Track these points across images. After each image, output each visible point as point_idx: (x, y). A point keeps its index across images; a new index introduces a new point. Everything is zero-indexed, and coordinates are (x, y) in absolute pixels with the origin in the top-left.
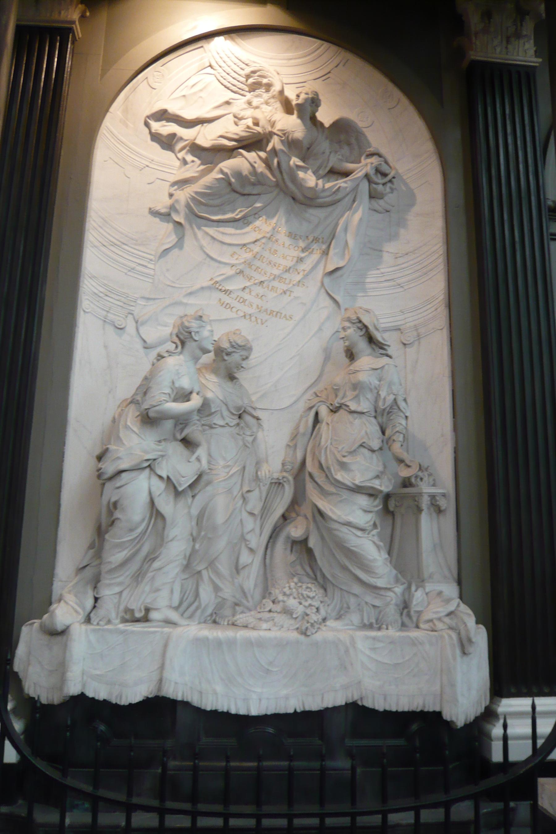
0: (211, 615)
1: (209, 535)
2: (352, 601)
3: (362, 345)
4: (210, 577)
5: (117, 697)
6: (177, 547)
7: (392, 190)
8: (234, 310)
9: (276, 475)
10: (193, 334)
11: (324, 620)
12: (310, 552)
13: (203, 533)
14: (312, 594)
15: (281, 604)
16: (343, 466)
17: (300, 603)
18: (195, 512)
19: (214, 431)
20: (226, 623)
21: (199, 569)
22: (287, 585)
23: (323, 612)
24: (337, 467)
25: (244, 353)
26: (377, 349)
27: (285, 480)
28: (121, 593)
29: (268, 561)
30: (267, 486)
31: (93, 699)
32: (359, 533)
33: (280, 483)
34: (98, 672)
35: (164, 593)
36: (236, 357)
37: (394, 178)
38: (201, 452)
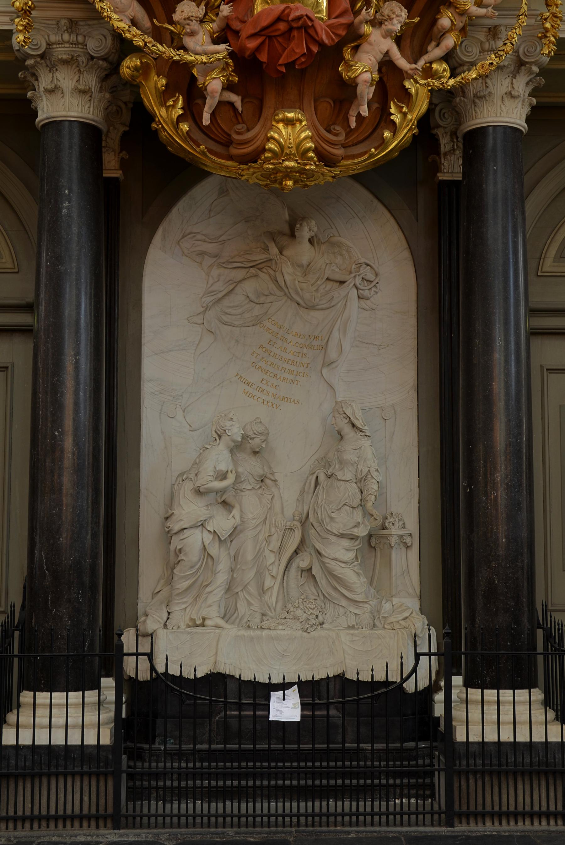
0: (246, 623)
1: (243, 568)
2: (342, 610)
3: (347, 430)
4: (244, 596)
5: (188, 674)
6: (222, 578)
7: (376, 293)
8: (256, 398)
9: (289, 524)
10: (227, 431)
11: (322, 624)
12: (314, 577)
13: (239, 567)
14: (313, 607)
15: (292, 613)
16: (332, 518)
17: (305, 612)
18: (232, 553)
19: (243, 493)
20: (256, 627)
21: (236, 591)
22: (297, 601)
23: (320, 618)
24: (328, 520)
25: (263, 438)
26: (358, 432)
27: (295, 526)
28: (186, 608)
29: (285, 584)
30: (283, 532)
31: (173, 675)
32: (343, 565)
33: (292, 529)
34: (175, 659)
35: (215, 608)
36: (257, 441)
37: (377, 283)
38: (236, 512)
